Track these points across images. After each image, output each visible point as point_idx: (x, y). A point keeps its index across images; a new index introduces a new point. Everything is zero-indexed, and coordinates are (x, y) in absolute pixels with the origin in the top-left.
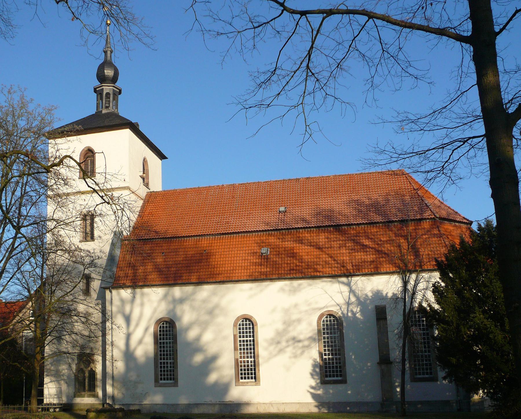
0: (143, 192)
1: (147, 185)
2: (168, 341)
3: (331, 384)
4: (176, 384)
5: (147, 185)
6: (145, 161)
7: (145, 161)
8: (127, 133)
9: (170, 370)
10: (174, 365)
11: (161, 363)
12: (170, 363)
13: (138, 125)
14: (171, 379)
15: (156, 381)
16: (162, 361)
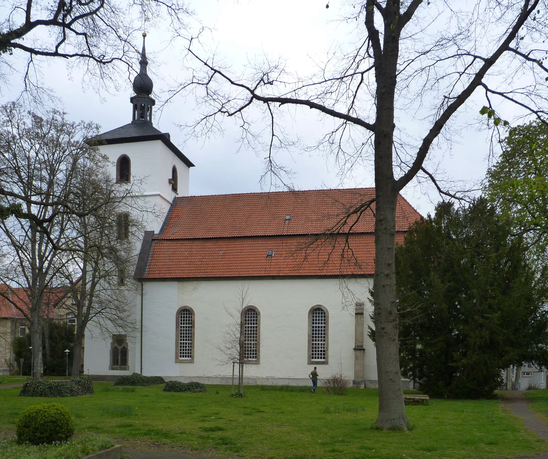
0: (170, 196)
1: (175, 189)
2: (187, 325)
3: (444, 398)
4: (192, 362)
5: (175, 189)
6: (174, 171)
7: (174, 171)
8: (158, 145)
9: (188, 350)
10: (192, 345)
11: (181, 343)
12: (189, 344)
13: (169, 136)
14: (188, 357)
15: (177, 358)
16: (182, 342)
